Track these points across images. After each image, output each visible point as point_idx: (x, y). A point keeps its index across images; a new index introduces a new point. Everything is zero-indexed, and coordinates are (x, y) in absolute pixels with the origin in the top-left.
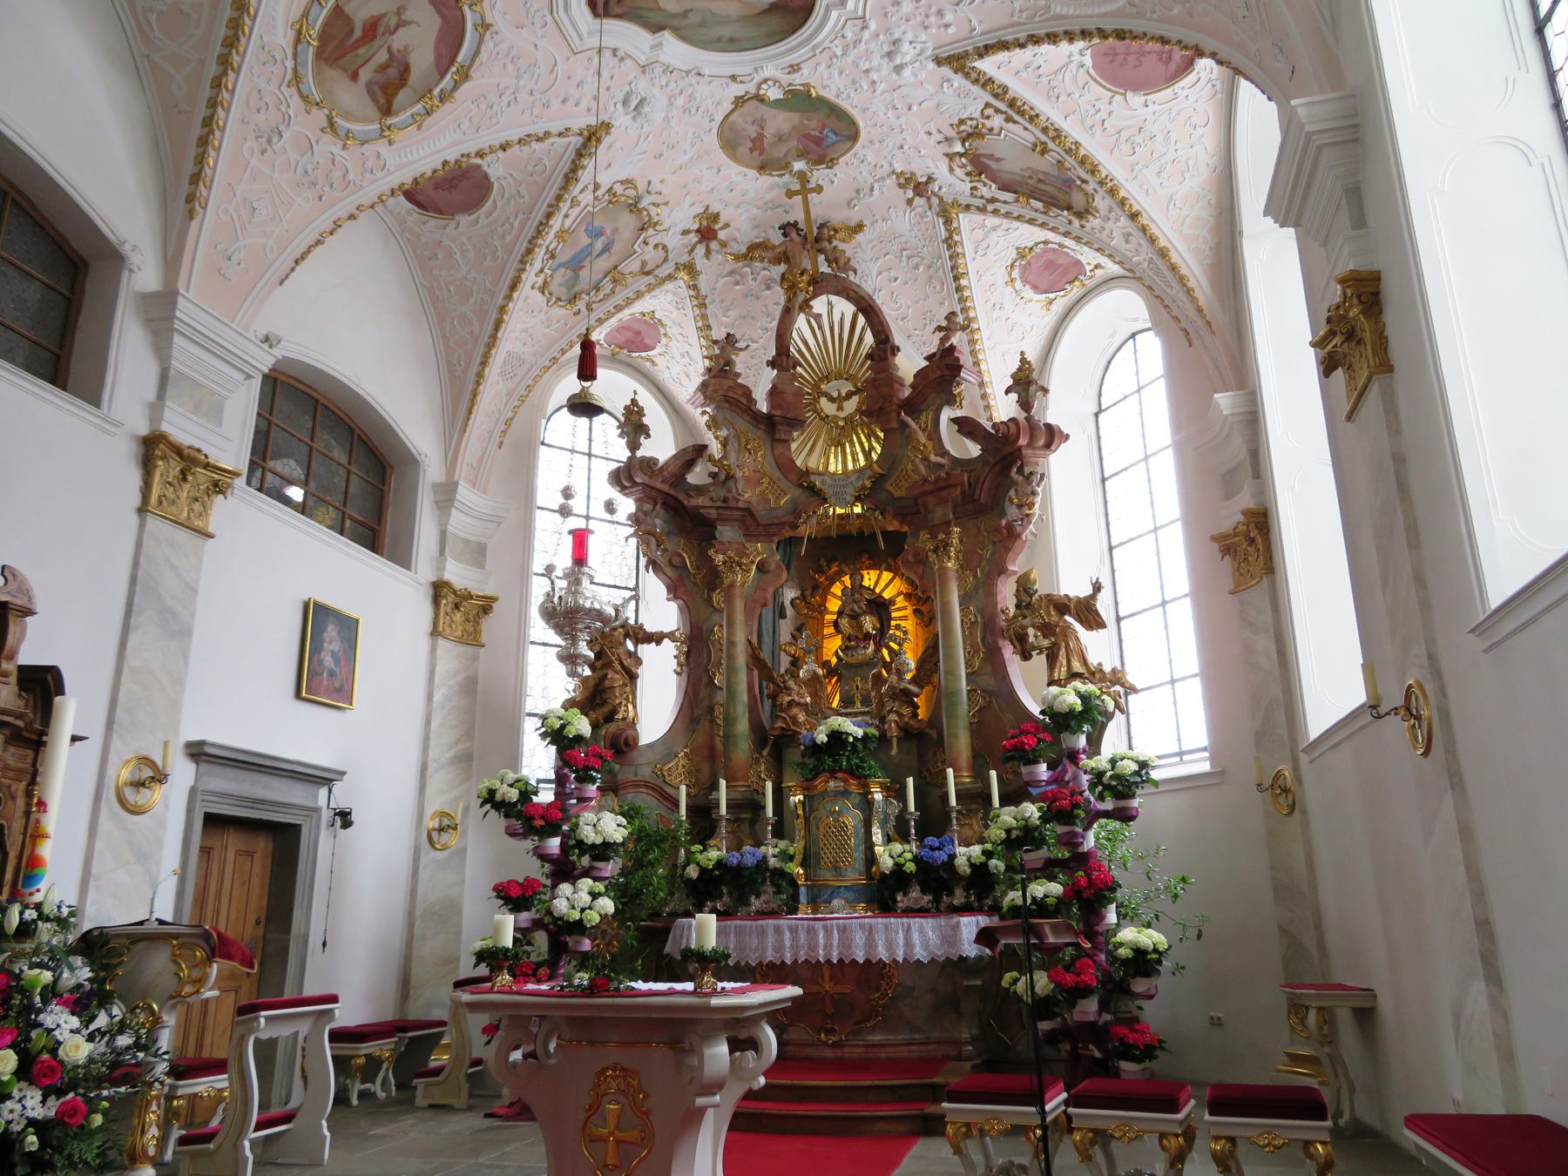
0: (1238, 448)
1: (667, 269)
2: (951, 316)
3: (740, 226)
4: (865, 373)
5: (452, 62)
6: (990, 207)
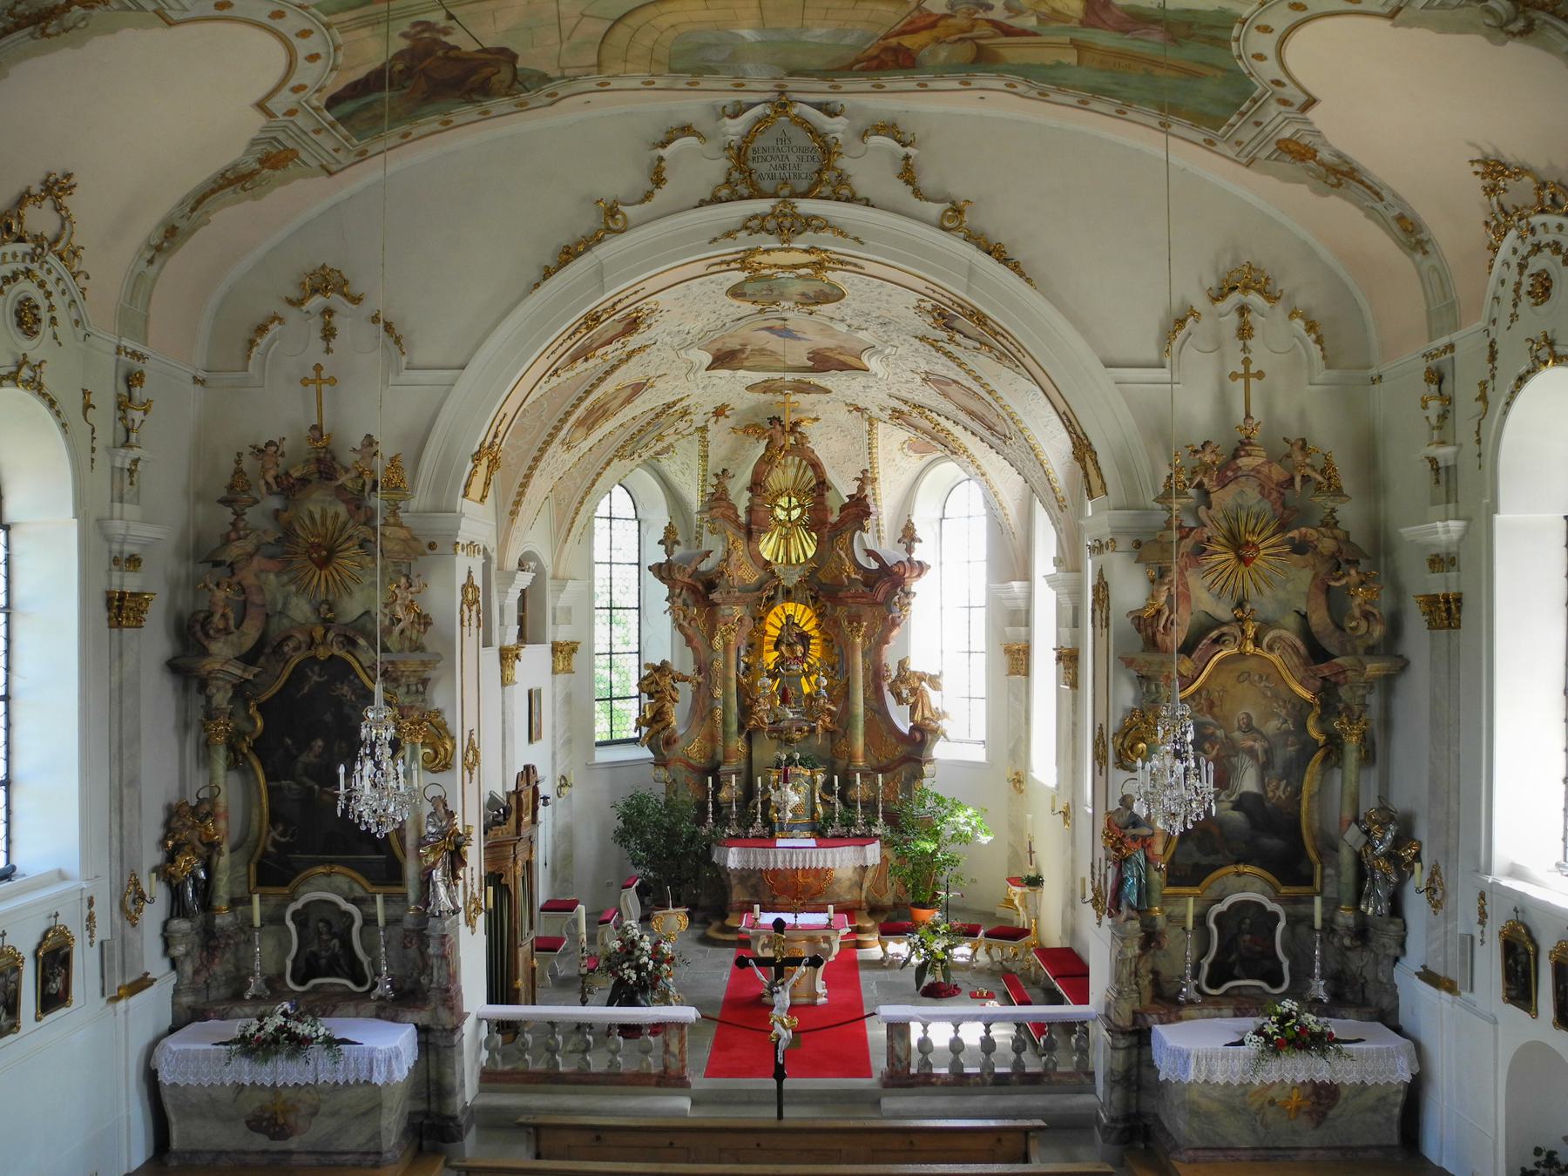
0: (1022, 604)
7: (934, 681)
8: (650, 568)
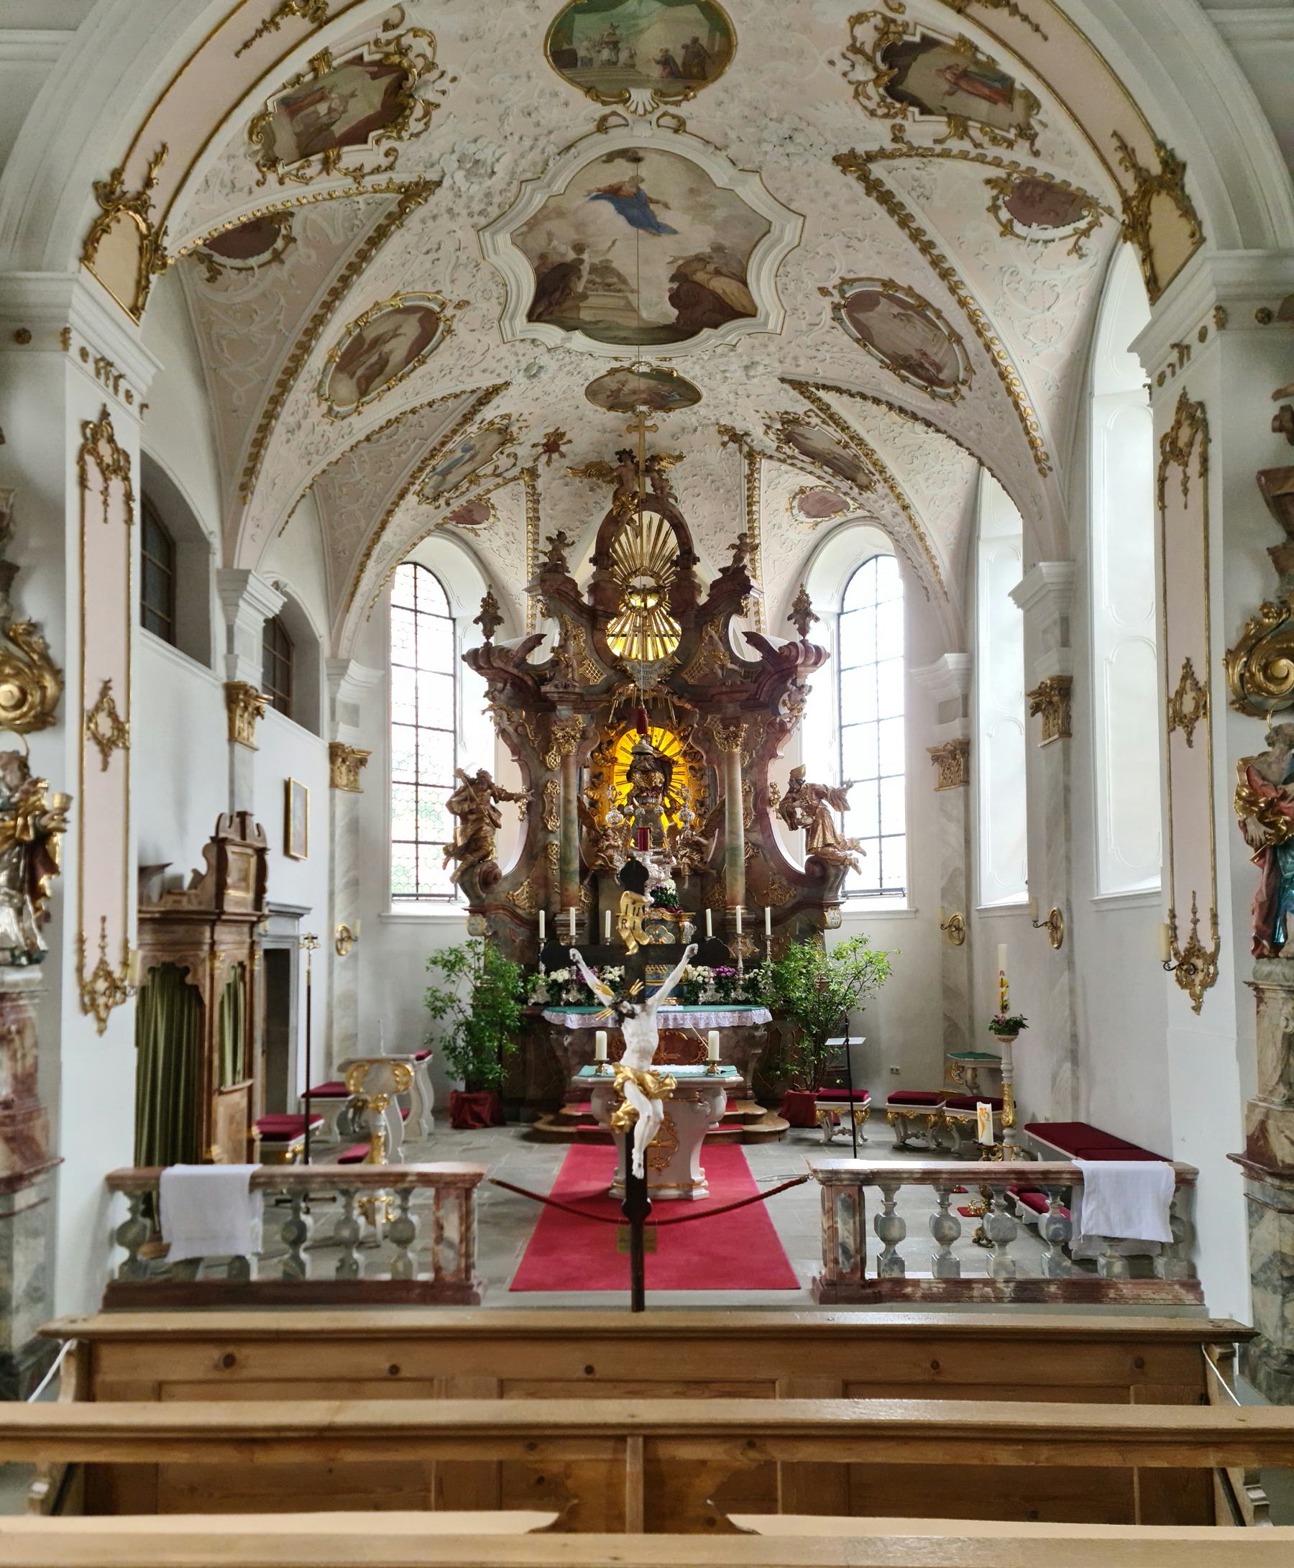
0: (956, 690)
1: (516, 471)
2: (742, 537)
3: (581, 444)
4: (669, 576)
5: (419, 353)
6: (789, 461)
7: (838, 799)
8: (464, 658)
